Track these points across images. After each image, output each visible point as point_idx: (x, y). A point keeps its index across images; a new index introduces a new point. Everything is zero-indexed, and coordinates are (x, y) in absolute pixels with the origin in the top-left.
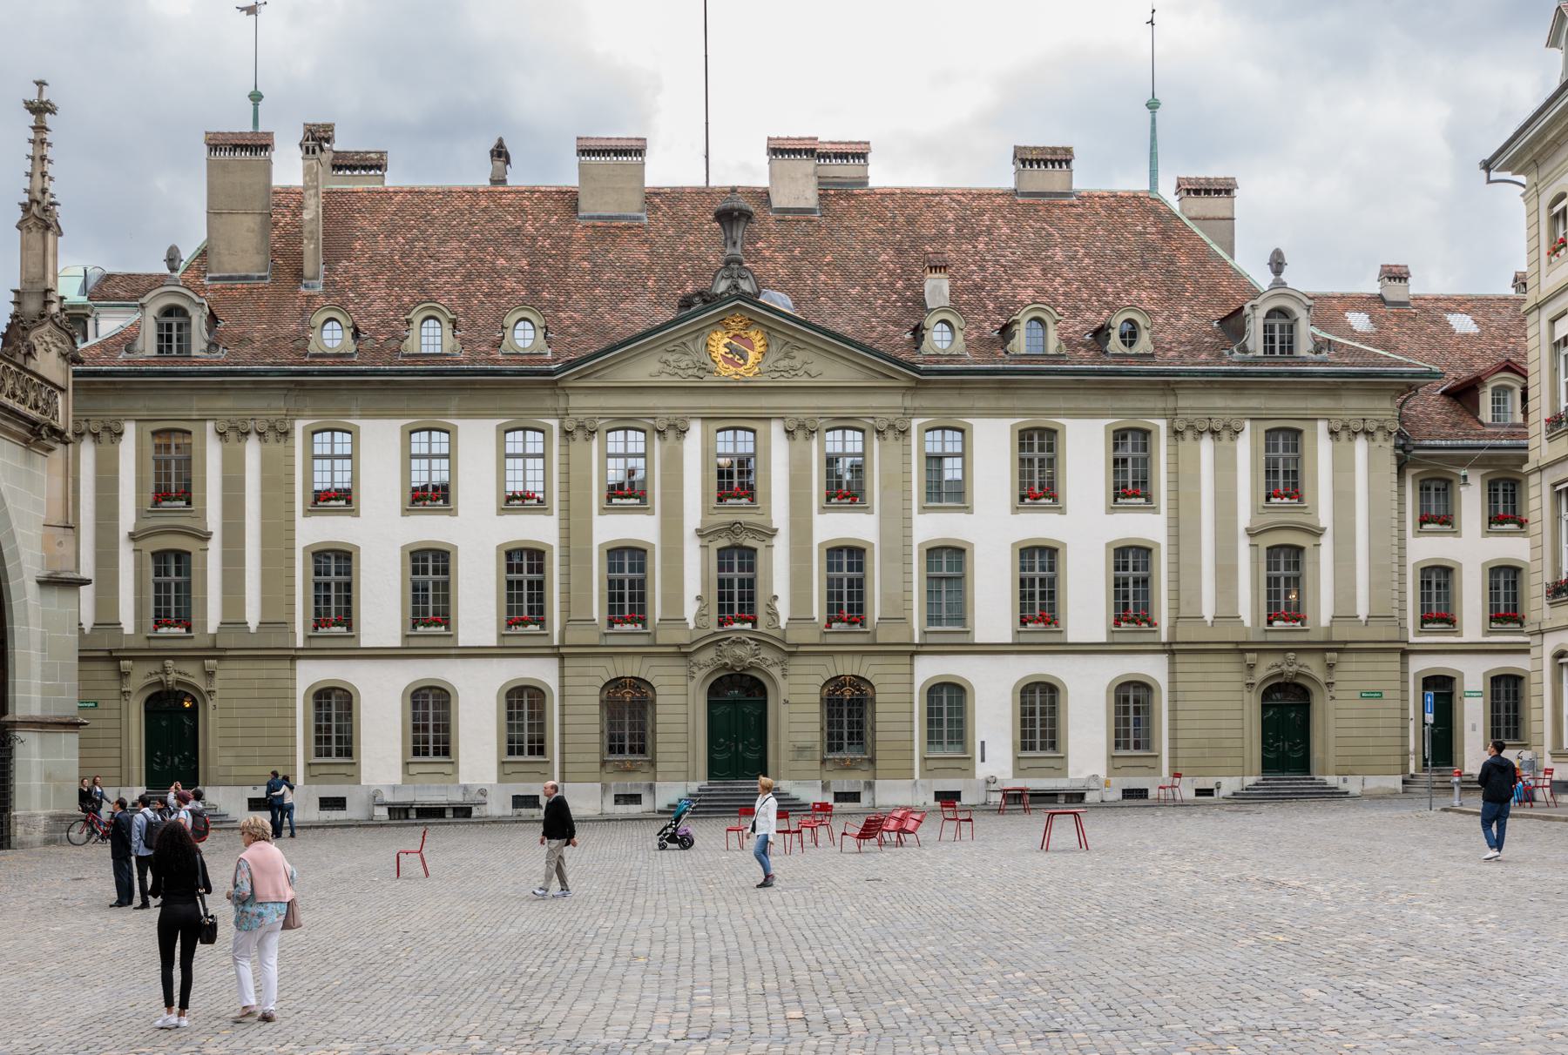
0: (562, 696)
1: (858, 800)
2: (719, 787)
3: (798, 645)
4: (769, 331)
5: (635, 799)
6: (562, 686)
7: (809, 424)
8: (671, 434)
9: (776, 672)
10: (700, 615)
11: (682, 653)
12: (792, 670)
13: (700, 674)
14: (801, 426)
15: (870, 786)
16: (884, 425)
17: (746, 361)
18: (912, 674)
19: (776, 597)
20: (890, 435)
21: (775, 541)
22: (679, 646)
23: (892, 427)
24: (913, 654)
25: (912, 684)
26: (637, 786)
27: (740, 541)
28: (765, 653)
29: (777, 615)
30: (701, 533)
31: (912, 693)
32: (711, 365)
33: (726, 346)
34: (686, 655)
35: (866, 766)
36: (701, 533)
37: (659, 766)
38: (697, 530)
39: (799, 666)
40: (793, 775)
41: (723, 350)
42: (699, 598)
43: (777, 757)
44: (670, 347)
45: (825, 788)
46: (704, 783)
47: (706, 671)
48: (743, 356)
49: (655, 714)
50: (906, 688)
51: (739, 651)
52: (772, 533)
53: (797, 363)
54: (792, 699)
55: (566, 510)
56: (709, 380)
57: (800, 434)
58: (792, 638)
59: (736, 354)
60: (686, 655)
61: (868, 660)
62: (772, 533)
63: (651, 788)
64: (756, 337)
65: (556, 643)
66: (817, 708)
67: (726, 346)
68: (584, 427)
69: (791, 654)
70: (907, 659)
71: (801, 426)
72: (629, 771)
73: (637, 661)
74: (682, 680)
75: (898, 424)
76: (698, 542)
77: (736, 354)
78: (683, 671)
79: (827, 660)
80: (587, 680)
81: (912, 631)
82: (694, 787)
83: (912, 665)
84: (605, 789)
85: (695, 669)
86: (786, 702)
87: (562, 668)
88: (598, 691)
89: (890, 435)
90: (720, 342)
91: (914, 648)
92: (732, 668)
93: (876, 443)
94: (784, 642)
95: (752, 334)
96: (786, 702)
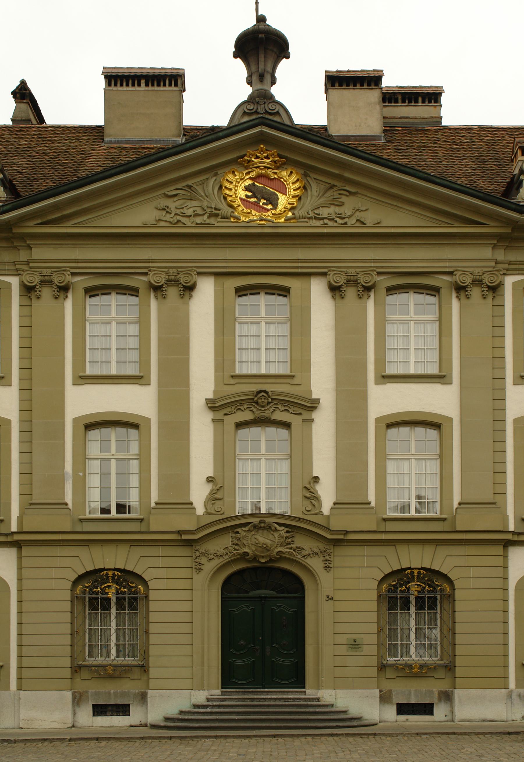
0: (20, 591)
1: (431, 713)
2: (235, 696)
3: (347, 532)
4: (306, 171)
5: (123, 710)
6: (20, 580)
7: (362, 279)
8: (172, 292)
9: (316, 564)
10: (213, 498)
11: (186, 541)
12: (337, 561)
13: (209, 567)
14: (352, 282)
15: (447, 697)
16: (468, 280)
17: (275, 206)
18: (505, 568)
19: (316, 479)
20: (476, 292)
21: (316, 415)
22: (179, 532)
23: (477, 282)
24: (507, 544)
25: (506, 579)
26: (124, 694)
27: (267, 414)
28: (299, 541)
29: (317, 498)
30: (212, 405)
31: (506, 590)
32: (225, 210)
33: (247, 189)
34: (189, 543)
35: (441, 673)
36: (212, 405)
37: (153, 672)
38: (208, 401)
39: (348, 559)
40: (340, 683)
41: (242, 194)
42: (210, 480)
43: (317, 662)
44: (170, 190)
45: (385, 698)
46: (217, 692)
47: (217, 562)
48: (273, 201)
49: (148, 611)
50: (498, 583)
51: (262, 538)
52: (313, 405)
53: (346, 210)
54: (338, 595)
55: (27, 380)
56: (220, 227)
57: (351, 293)
58: (335, 525)
59: (262, 194)
60: (189, 543)
61: (443, 551)
62: (313, 405)
63: (143, 697)
64: (291, 180)
65: (14, 529)
66: (374, 605)
67: (247, 189)
68: (50, 283)
69: (337, 543)
70: (499, 550)
71: (352, 282)
72: (111, 677)
73: (123, 550)
74: (185, 573)
75: (486, 279)
76: (209, 416)
77: (262, 194)
78: (188, 562)
79: (388, 551)
80: (54, 573)
81: (505, 518)
82: (200, 697)
83: (505, 557)
84: (78, 700)
85: (204, 560)
86: (330, 598)
87: (20, 558)
88: (69, 585)
89: (476, 292)
90: (238, 187)
91: (509, 537)
92: (255, 559)
93: (455, 304)
94: (327, 529)
95: (284, 174)
96: (330, 598)
